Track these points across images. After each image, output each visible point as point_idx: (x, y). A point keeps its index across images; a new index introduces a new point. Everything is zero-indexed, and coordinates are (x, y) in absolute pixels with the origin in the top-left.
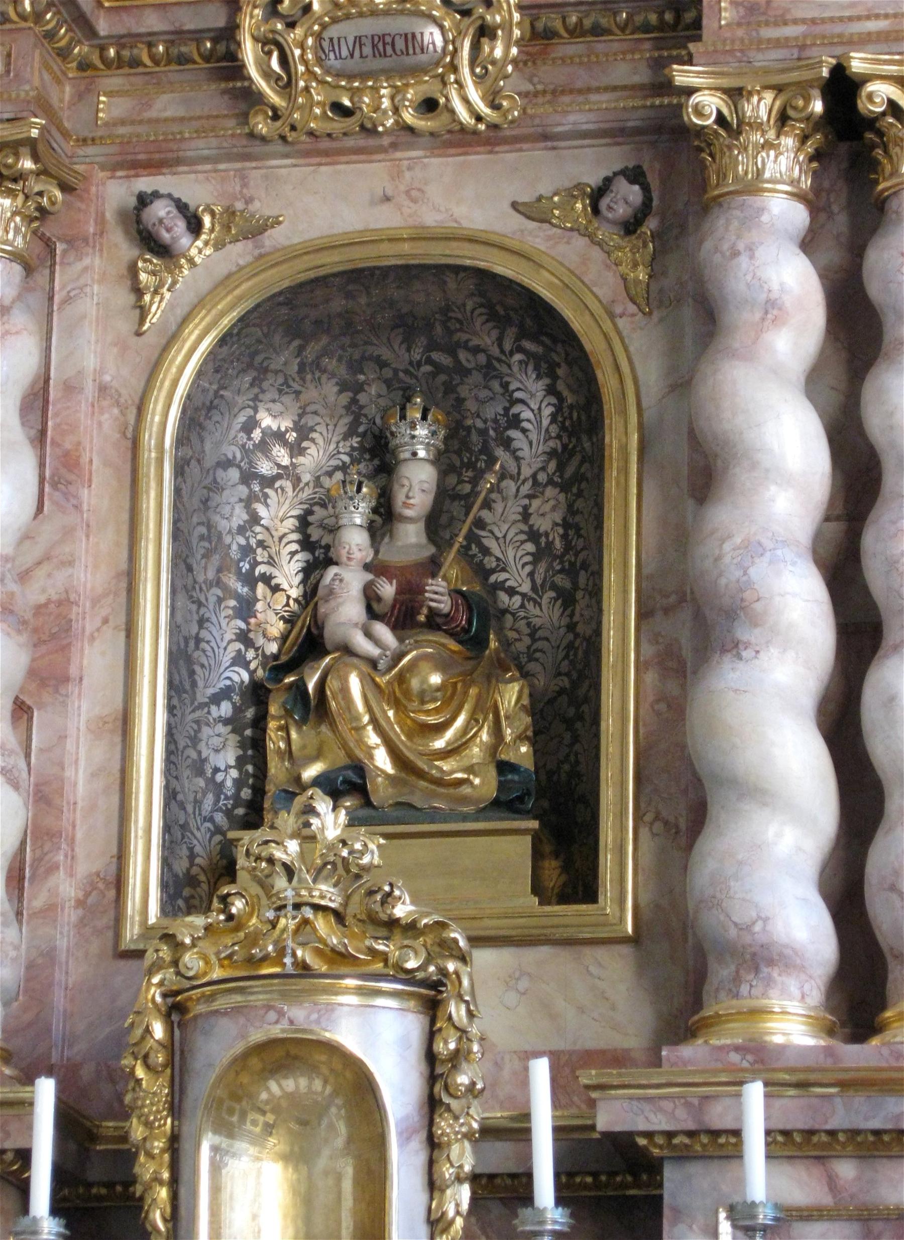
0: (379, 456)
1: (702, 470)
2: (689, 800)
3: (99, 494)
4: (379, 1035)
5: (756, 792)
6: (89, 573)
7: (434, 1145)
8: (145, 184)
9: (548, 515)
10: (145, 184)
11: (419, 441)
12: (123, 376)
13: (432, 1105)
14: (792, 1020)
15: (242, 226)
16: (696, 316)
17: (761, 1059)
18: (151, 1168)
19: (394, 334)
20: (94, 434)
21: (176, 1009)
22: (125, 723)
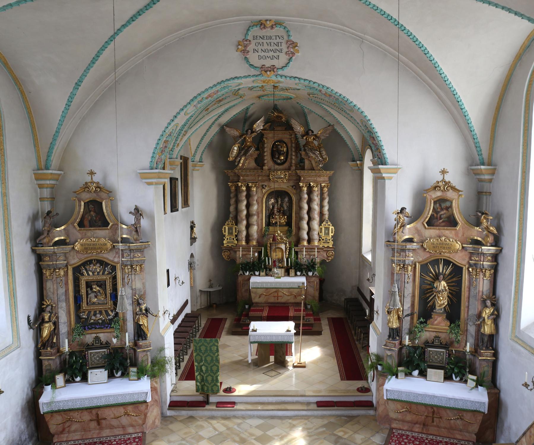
0: (277, 202)
1: (300, 208)
2: (299, 228)
3: (260, 204)
4: (283, 246)
5: (304, 229)
6: (260, 210)
7: (286, 253)
8: (263, 184)
9: (288, 204)
10: (263, 184)
11: (279, 200)
12: (261, 196)
13: (286, 250)
14: (305, 243)
15: (269, 186)
16: (300, 199)
17: (304, 246)
18: (269, 253)
19: (279, 194)
20: (260, 200)
21: (270, 244)
22: (262, 219)
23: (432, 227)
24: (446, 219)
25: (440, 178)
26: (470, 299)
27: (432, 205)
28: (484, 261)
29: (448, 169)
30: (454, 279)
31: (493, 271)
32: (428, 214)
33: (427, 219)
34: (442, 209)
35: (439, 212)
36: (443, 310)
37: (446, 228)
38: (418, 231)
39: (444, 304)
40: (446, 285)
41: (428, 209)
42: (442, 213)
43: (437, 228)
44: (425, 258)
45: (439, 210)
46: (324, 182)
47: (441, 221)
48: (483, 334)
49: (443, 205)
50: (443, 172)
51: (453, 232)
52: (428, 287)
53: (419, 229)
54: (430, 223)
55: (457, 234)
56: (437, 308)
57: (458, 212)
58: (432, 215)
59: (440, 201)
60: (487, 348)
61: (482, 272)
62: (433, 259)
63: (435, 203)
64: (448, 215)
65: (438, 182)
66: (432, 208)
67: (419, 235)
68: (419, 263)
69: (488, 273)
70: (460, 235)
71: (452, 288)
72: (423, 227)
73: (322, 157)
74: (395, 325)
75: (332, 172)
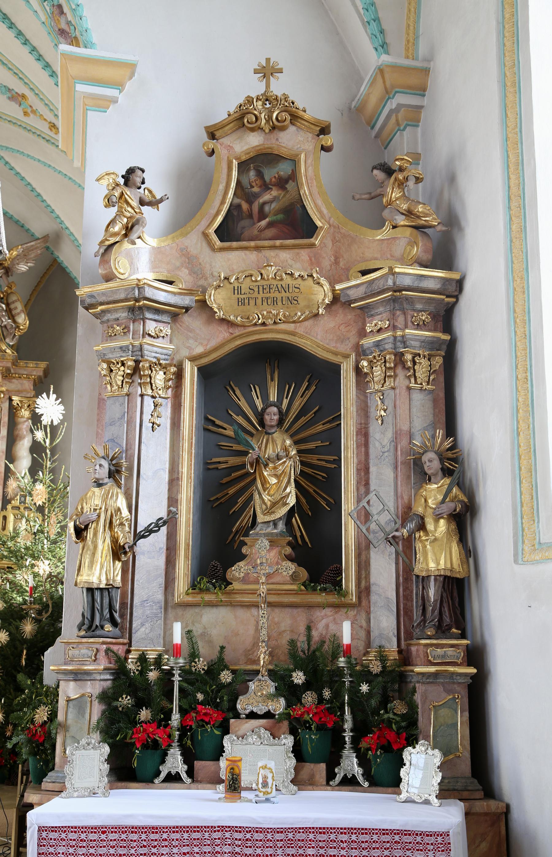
23: (235, 244)
24: (280, 216)
25: (257, 88)
26: (372, 469)
27: (235, 173)
28: (406, 327)
29: (279, 58)
30: (320, 427)
31: (438, 361)
32: (223, 202)
33: (220, 219)
34: (266, 187)
35: (256, 196)
36: (281, 526)
37: (278, 242)
38: (190, 260)
39: (282, 501)
40: (288, 442)
41: (222, 187)
42: (266, 197)
43: (252, 244)
44: (213, 343)
45: (256, 189)
46: (18, 392)
47: (263, 223)
48: (425, 580)
49: (270, 174)
50: (267, 71)
51: (304, 254)
52: (233, 461)
53: (193, 251)
54: (227, 232)
55: (315, 261)
56: (261, 518)
57: (315, 190)
58: (234, 209)
59: (258, 162)
60: (442, 630)
61: (404, 367)
62: (239, 342)
63: (243, 166)
64: (285, 201)
65: (250, 100)
66: (233, 184)
67: (192, 272)
68: (192, 359)
69: (422, 370)
70: (327, 263)
71: (313, 459)
72: (205, 244)
73: (12, 317)
74: (100, 570)
75: (43, 365)
